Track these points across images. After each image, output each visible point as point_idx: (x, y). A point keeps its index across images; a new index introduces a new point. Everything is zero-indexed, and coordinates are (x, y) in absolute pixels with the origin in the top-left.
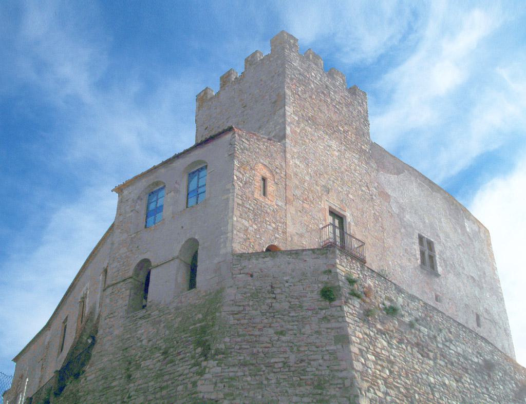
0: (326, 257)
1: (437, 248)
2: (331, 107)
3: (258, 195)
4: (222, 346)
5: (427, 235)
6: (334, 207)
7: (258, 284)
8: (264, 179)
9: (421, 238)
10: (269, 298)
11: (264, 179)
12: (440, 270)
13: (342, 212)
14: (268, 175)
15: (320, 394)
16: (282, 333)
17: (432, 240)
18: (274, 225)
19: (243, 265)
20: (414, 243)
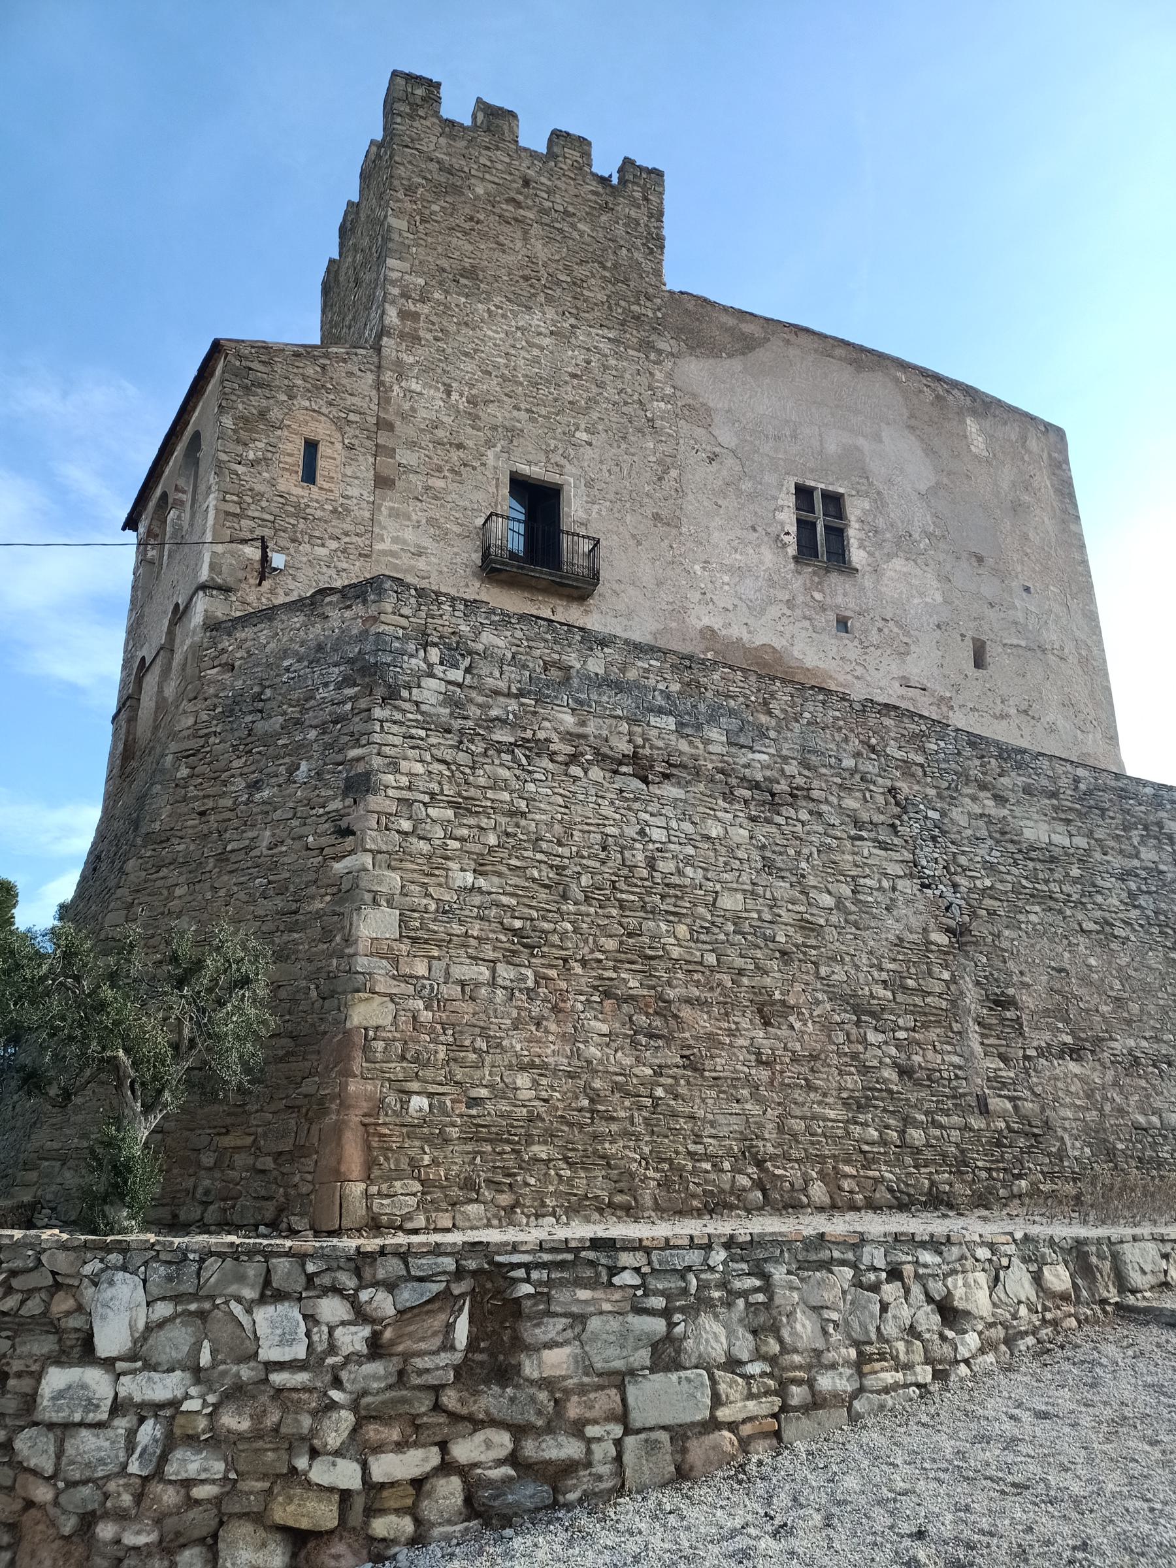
0: (365, 602)
1: (855, 510)
2: (536, 229)
3: (291, 484)
4: (157, 826)
5: (819, 485)
6: (525, 469)
7: (239, 684)
8: (311, 447)
9: (803, 494)
10: (251, 712)
11: (311, 447)
12: (857, 556)
13: (556, 478)
14: (321, 430)
15: (296, 912)
16: (255, 786)
17: (841, 490)
18: (334, 545)
19: (220, 646)
20: (780, 509)
